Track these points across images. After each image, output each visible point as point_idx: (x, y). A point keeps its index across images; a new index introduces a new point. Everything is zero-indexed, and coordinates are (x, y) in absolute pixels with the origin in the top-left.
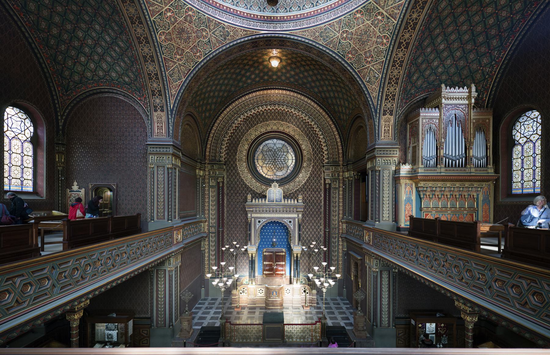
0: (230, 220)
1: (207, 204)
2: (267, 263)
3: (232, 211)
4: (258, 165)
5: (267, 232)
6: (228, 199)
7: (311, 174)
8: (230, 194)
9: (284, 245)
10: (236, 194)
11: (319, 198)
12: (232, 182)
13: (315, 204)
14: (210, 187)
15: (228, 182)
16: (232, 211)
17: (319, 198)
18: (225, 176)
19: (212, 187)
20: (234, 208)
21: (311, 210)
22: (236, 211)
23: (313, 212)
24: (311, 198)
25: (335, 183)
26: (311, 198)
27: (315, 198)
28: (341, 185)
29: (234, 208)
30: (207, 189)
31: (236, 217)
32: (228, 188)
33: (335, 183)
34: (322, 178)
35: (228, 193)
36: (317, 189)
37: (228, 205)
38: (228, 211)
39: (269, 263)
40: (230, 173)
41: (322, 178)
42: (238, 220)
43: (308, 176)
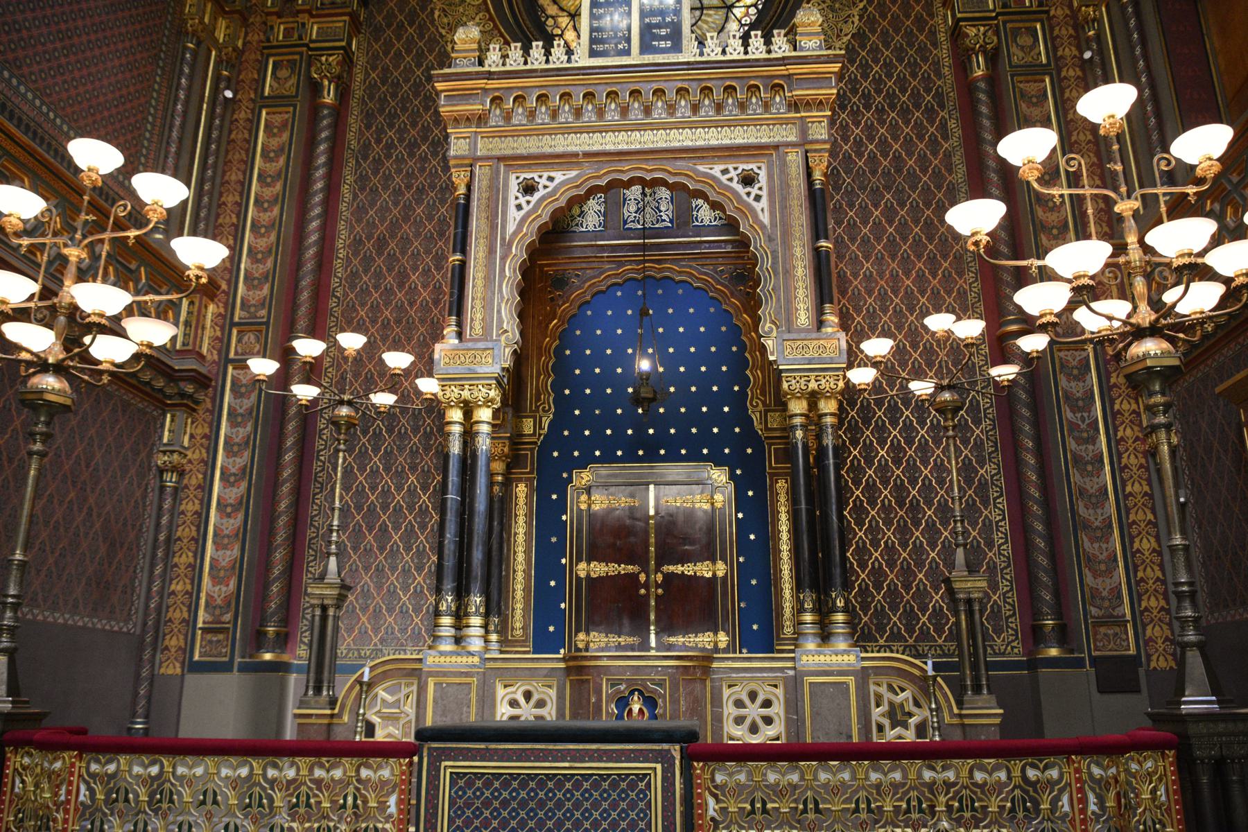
0: (365, 292)
1: (230, 199)
2: (599, 569)
3: (381, 244)
4: (552, 10)
5: (599, 358)
6: (362, 180)
7: (871, 23)
8: (377, 150)
9: (716, 445)
10: (413, 146)
11: (934, 143)
12: (397, 85)
13: (913, 180)
14: (262, 102)
15: (371, 89)
16: (381, 244)
17: (934, 144)
18: (361, 60)
19: (276, 101)
20: (394, 227)
21: (890, 214)
22: (405, 241)
23: (903, 230)
24: (884, 146)
25: (1025, 40)
26: (884, 146)
27: (908, 143)
28: (1068, 52)
29: (394, 227)
30: (242, 115)
31: (402, 278)
32: (369, 117)
33: (1025, 40)
34: (942, 37)
35: (366, 147)
36: (916, 97)
37: (359, 212)
38: (357, 244)
39: (613, 569)
40: (388, 45)
41: (942, 37)
42: (413, 291)
43: (850, 29)
